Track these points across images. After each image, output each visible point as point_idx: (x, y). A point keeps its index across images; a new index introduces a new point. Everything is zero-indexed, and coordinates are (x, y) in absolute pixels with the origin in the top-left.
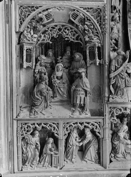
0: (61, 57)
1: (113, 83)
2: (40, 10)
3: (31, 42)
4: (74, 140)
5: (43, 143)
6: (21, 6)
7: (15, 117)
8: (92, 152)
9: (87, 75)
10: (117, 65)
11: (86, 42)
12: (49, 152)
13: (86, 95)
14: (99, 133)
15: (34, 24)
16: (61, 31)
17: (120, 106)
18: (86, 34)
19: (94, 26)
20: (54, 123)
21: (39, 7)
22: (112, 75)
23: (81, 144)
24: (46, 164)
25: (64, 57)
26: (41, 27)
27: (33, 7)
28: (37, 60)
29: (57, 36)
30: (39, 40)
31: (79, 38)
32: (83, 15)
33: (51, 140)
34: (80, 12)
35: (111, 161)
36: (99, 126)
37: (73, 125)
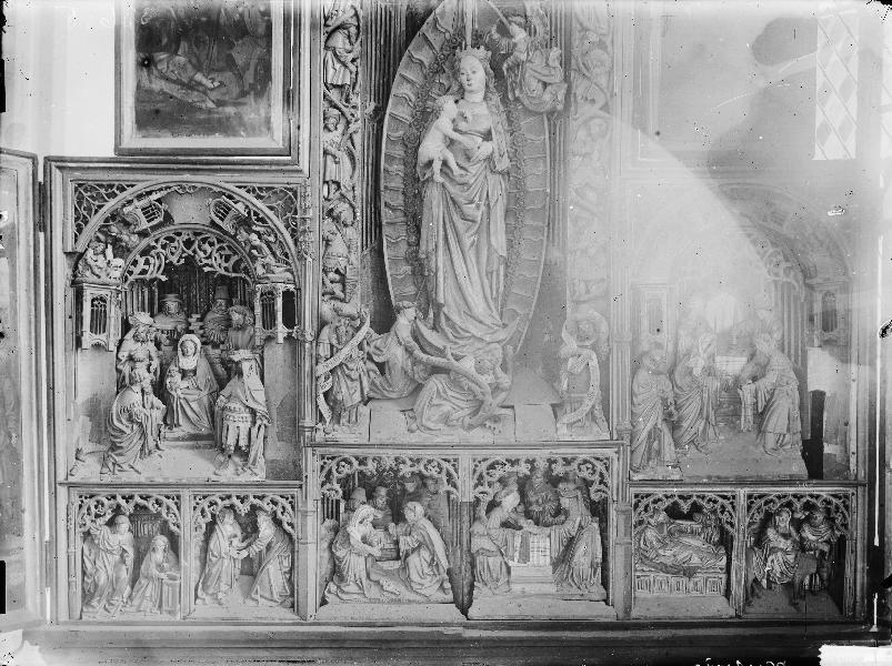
0: (199, 316)
1: (327, 389)
2: (128, 194)
3: (104, 279)
4: (225, 544)
5: (142, 551)
6: (80, 185)
7: (61, 478)
8: (274, 572)
9: (263, 364)
10: (334, 342)
11: (258, 280)
12: (155, 572)
13: (254, 423)
14: (290, 524)
15: (115, 230)
16: (193, 248)
17: (348, 453)
18: (254, 259)
19: (276, 237)
20: (168, 497)
21: (128, 186)
22: (322, 369)
23: (244, 554)
24: (147, 604)
25: (209, 316)
26: (135, 238)
27: (111, 186)
28: (126, 327)
29: (182, 261)
30: (131, 273)
31: (242, 265)
32: (247, 207)
33: (161, 542)
34: (237, 198)
35: (324, 602)
36: (293, 508)
37: (219, 501)
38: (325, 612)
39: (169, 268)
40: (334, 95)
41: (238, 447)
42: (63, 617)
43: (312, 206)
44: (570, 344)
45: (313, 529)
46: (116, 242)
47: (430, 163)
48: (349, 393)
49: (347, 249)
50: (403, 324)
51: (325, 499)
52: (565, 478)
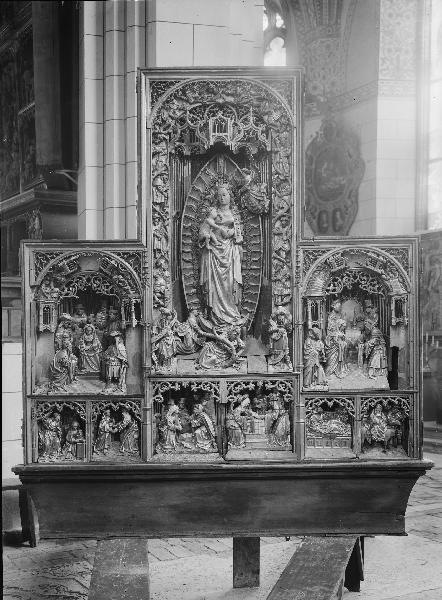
8: (131, 437)
17: (165, 380)
35: (155, 453)
38: (156, 457)
39: (79, 292)
40: (157, 208)
41: (113, 378)
42: (30, 461)
43: (150, 261)
44: (274, 325)
45: (150, 419)
46: (55, 280)
47: (204, 239)
48: (166, 352)
49: (165, 284)
50: (192, 319)
51: (155, 403)
52: (273, 391)
